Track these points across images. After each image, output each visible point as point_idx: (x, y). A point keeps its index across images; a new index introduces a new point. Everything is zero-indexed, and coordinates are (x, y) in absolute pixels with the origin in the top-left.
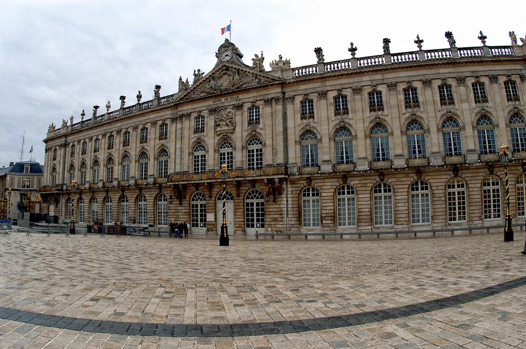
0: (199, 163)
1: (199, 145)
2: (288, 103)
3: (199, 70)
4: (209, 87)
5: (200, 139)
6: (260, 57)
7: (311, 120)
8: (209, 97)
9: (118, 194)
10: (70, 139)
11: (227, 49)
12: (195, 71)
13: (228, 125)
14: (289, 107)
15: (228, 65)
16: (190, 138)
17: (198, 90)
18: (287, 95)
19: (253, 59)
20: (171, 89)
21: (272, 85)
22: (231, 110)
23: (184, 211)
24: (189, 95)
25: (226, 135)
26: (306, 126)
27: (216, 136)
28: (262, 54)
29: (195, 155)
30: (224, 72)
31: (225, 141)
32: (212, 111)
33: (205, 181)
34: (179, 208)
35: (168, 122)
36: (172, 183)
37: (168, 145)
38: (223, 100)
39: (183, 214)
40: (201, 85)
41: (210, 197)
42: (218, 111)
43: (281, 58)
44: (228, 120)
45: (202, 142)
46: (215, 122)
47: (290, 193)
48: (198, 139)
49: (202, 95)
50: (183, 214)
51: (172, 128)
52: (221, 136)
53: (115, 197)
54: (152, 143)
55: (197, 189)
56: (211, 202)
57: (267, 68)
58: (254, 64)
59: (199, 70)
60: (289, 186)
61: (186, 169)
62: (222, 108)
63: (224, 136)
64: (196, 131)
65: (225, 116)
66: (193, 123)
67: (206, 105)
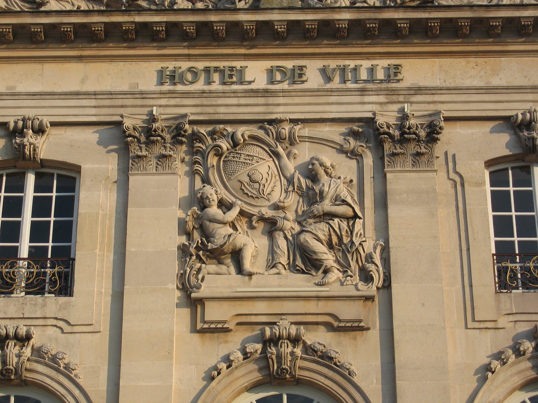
5: (24, 340)
13: (309, 262)
22: (328, 157)
25: (295, 340)
38: (256, 72)
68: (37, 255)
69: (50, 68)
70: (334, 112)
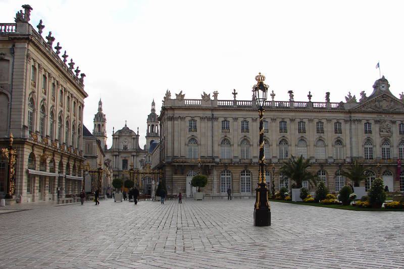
1: (369, 141)
10: (216, 114)
16: (362, 137)
20: (338, 98)
31: (386, 141)
32: (377, 122)
38: (383, 116)
46: (379, 129)
51: (345, 127)
52: (384, 138)
58: (401, 97)
64: (366, 132)
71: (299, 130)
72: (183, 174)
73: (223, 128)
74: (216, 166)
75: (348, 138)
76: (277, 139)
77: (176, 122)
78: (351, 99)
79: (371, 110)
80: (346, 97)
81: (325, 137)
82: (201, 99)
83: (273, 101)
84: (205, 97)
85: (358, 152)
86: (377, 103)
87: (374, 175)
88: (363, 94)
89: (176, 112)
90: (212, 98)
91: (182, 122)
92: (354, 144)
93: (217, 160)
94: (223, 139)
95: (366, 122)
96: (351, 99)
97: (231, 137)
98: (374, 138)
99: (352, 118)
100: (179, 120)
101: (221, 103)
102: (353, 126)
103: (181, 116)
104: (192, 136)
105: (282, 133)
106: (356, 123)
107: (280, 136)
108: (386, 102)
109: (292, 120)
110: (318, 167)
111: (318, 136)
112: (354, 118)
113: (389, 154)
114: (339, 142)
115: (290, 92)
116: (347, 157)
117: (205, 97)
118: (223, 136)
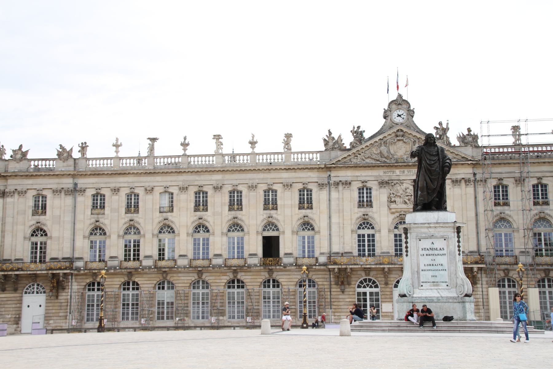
0: (367, 244)
2: (479, 186)
3: (359, 127)
4: (376, 152)
5: (367, 215)
6: (444, 126)
7: (506, 208)
8: (379, 166)
9: (225, 277)
10: (82, 182)
11: (400, 107)
12: (354, 128)
13: (406, 203)
14: (480, 190)
15: (405, 130)
17: (362, 154)
18: (478, 177)
19: (436, 128)
21: (462, 164)
23: (348, 300)
24: (349, 158)
26: (501, 213)
27: (390, 214)
28: (448, 124)
29: (359, 233)
30: (400, 138)
32: (383, 184)
33: (385, 266)
34: (340, 297)
35: (314, 187)
36: (336, 267)
37: (315, 217)
38: (398, 172)
39: (347, 303)
40: (367, 148)
41: (386, 284)
42: (393, 184)
43: (469, 130)
44: (407, 198)
45: (370, 219)
47: (484, 283)
48: (364, 215)
49: (368, 161)
50: (347, 303)
51: (319, 197)
52: (398, 214)
53: (218, 281)
54: (288, 212)
55: (368, 274)
56: (388, 290)
57: (454, 141)
59: (359, 127)
60: (484, 275)
61: (348, 249)
62: (398, 182)
63: (401, 215)
64: (361, 204)
65: (401, 192)
66: (356, 195)
67: (373, 174)
68: (367, 201)
69: (367, 171)
70: (409, 178)
71: (230, 205)
72: (15, 290)
73: (94, 207)
74: (77, 275)
75: (325, 217)
76: (189, 224)
77: (9, 200)
78: (332, 144)
79: (373, 162)
80: (325, 140)
81: (279, 217)
82: (57, 157)
83: (185, 155)
84: (64, 154)
85: (346, 242)
86: (383, 148)
87: (376, 286)
88: (358, 134)
89: (10, 181)
90: (76, 155)
91: (22, 200)
92: (334, 229)
93: (80, 264)
94: (93, 226)
95: (360, 185)
96: (332, 144)
97: (106, 222)
98: (376, 216)
99: (333, 179)
100: (16, 195)
101: (92, 164)
102: (334, 194)
103: (19, 188)
104: (37, 223)
105: (198, 213)
106: (341, 187)
107: (195, 218)
108: (404, 145)
109: (217, 188)
110: (263, 273)
111: (265, 216)
112: (337, 179)
113: (43, 252)
114: (307, 225)
115: (217, 137)
116: (322, 254)
117: (64, 154)
118: (93, 220)
